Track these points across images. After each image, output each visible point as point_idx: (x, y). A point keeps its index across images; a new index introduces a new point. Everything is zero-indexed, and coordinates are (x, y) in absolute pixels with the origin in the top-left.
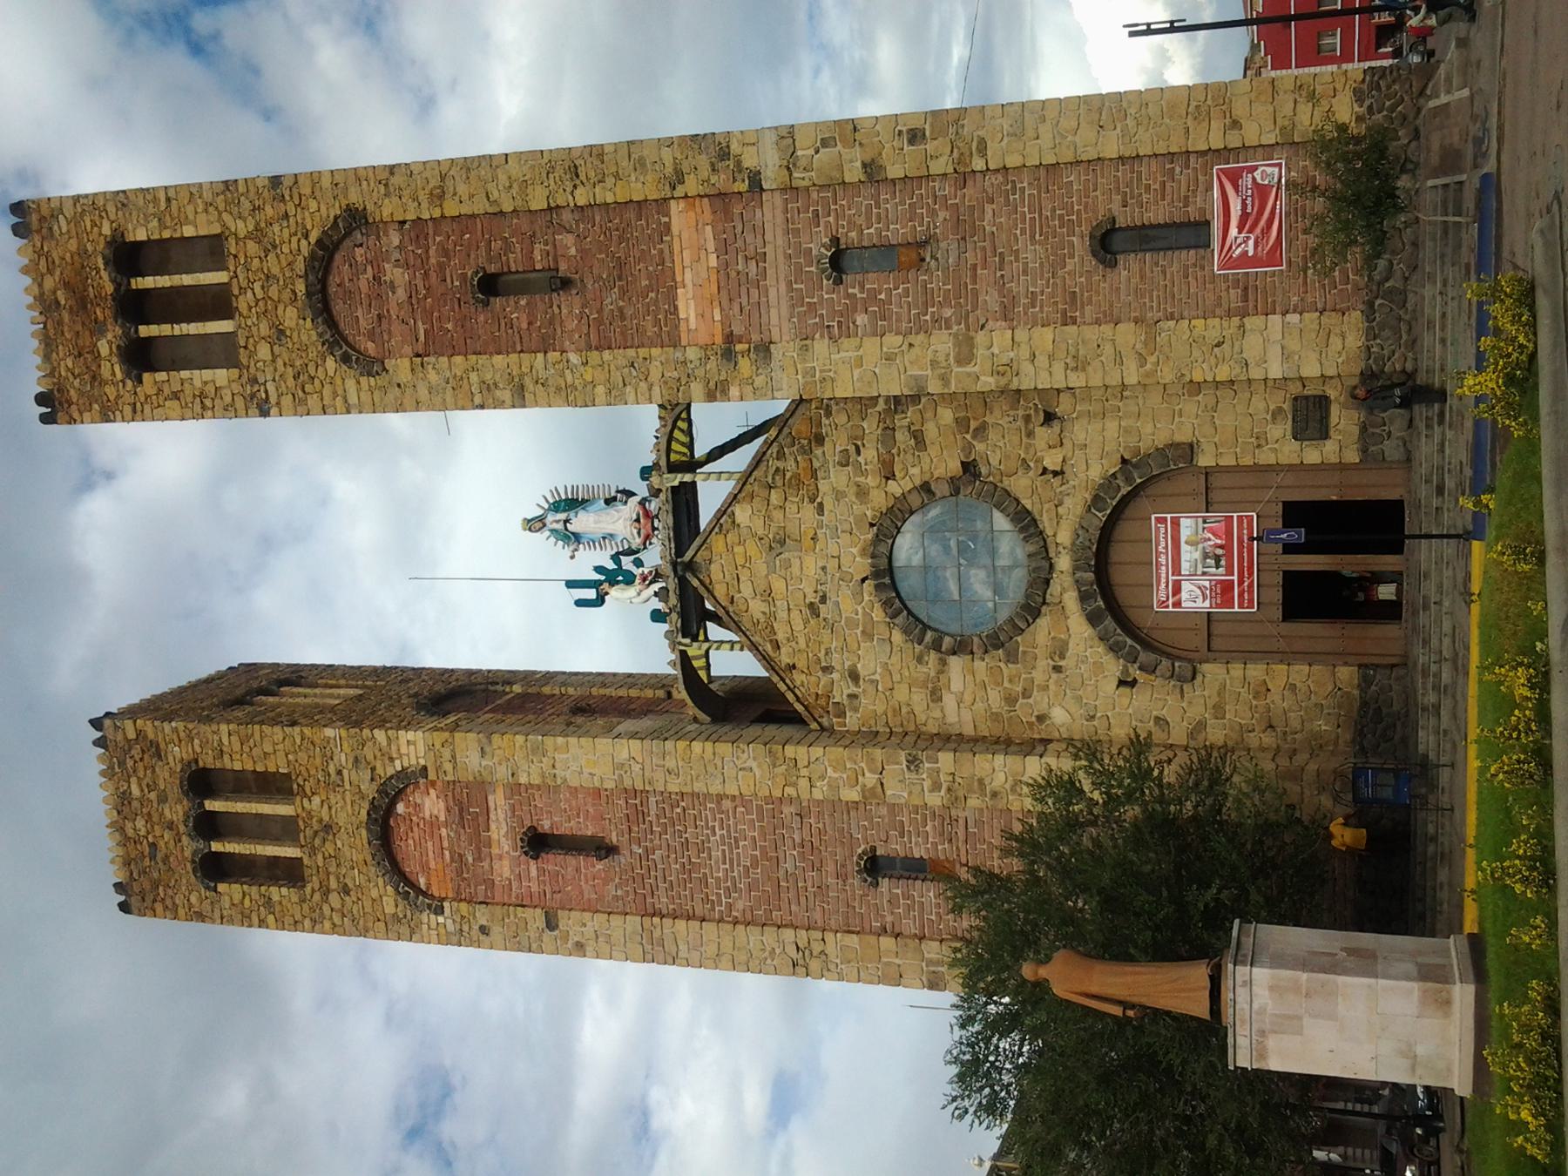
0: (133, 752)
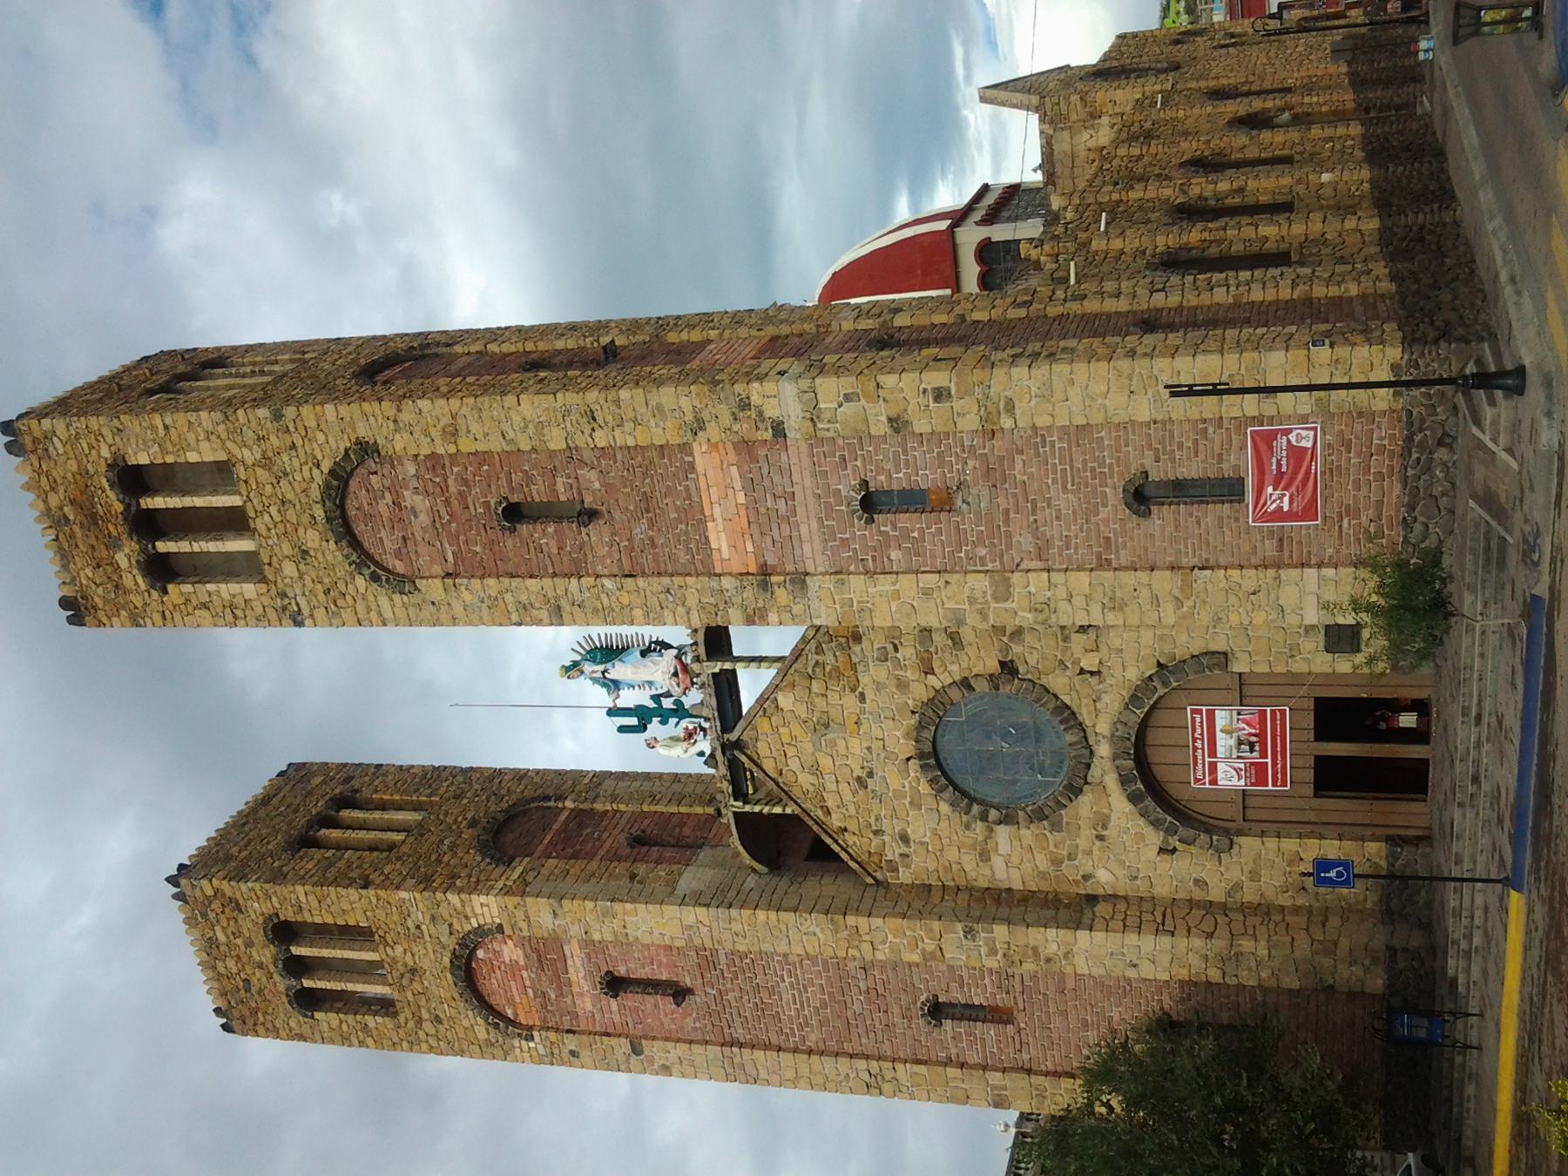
0: (213, 907)
